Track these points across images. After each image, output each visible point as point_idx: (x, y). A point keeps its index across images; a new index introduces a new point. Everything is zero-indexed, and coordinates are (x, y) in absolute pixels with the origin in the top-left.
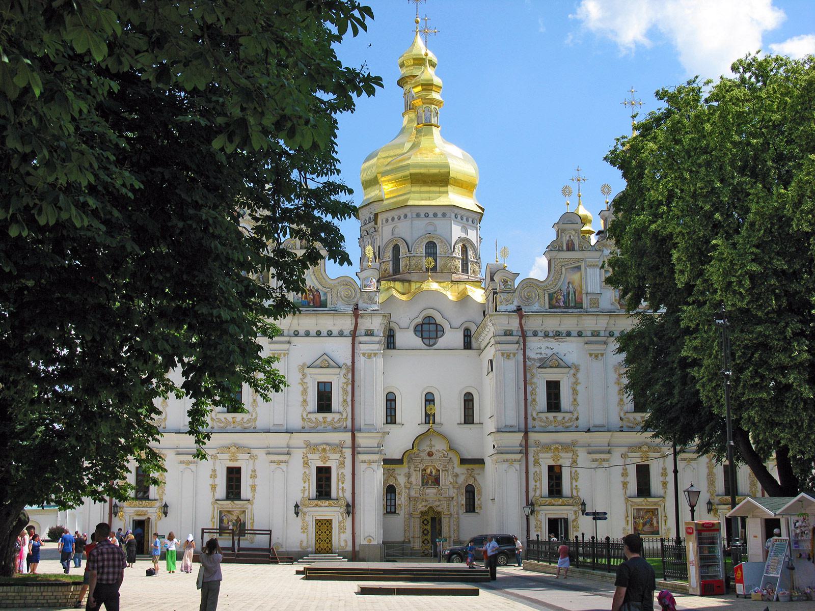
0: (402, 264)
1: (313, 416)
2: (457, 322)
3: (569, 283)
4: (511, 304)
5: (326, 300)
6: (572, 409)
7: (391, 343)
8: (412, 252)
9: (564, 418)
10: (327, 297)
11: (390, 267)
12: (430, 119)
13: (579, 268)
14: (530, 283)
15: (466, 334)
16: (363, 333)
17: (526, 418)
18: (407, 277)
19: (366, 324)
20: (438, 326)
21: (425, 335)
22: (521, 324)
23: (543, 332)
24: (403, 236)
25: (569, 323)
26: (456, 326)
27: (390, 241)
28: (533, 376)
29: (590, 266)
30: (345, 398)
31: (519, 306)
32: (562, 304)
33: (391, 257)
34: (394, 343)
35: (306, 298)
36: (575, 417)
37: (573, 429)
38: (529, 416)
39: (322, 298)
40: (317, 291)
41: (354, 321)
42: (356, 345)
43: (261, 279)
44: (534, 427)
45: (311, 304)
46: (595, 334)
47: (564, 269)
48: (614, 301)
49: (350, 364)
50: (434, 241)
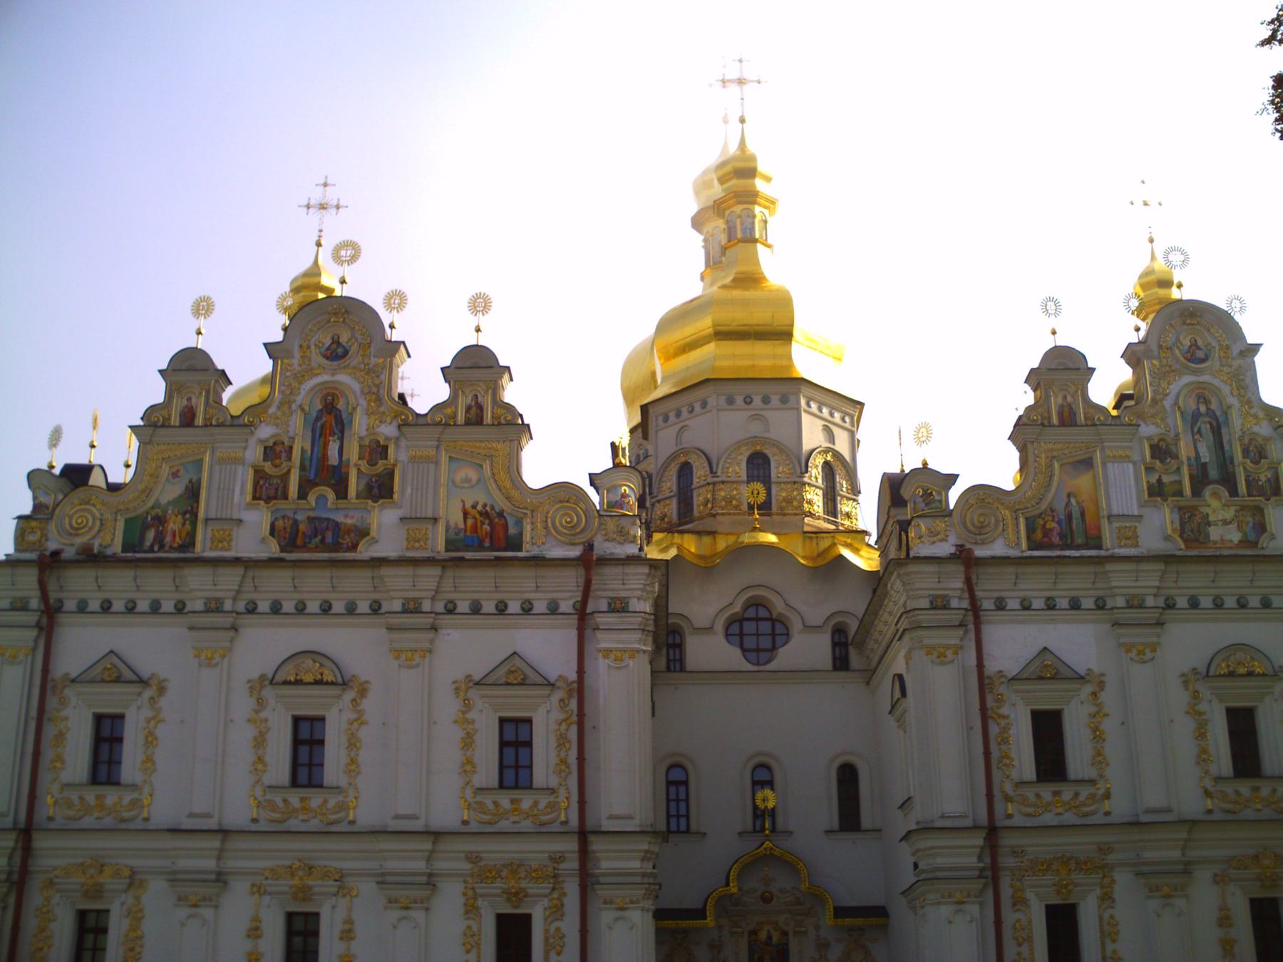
0: (698, 499)
1: (488, 800)
2: (816, 615)
3: (1069, 495)
4: (941, 540)
5: (521, 534)
6: (1092, 773)
7: (674, 660)
8: (719, 474)
9: (1077, 795)
10: (522, 527)
11: (672, 508)
12: (752, 229)
13: (1088, 463)
14: (982, 494)
15: (836, 640)
16: (604, 607)
17: (990, 796)
18: (709, 524)
19: (611, 583)
20: (778, 626)
21: (750, 642)
22: (968, 581)
23: (1018, 601)
24: (696, 445)
25: (1076, 582)
26: (820, 622)
27: (673, 457)
28: (1000, 701)
29: (1115, 459)
30: (563, 754)
31: (962, 546)
32: (1056, 540)
33: (674, 488)
34: (682, 661)
35: (475, 529)
36: (1101, 792)
37: (1098, 819)
38: (996, 792)
39: (512, 531)
40: (501, 514)
41: (582, 580)
42: (588, 632)
43: (376, 491)
44: (1009, 816)
45: (487, 544)
46: (1136, 603)
47: (1056, 465)
48: (1169, 532)
49: (573, 676)
50: (766, 452)
